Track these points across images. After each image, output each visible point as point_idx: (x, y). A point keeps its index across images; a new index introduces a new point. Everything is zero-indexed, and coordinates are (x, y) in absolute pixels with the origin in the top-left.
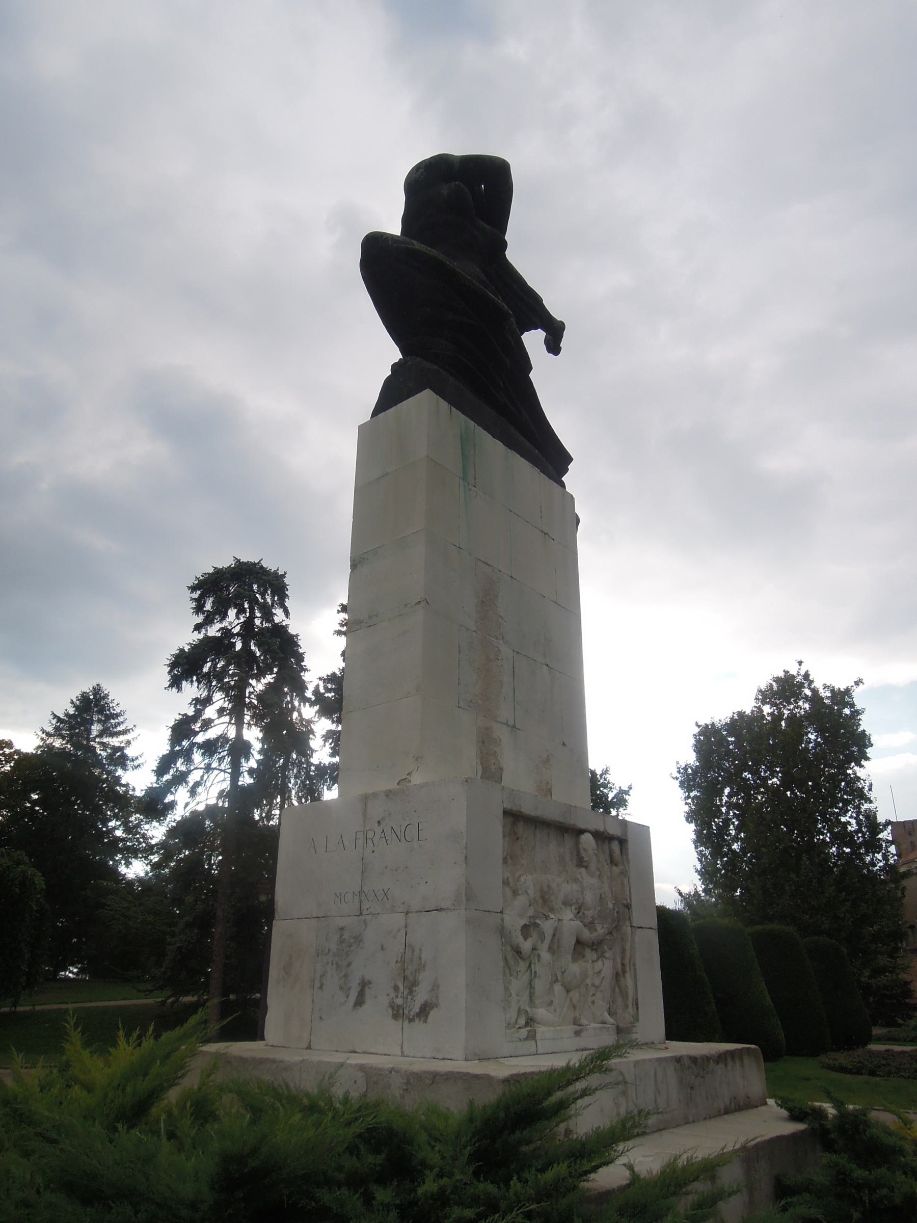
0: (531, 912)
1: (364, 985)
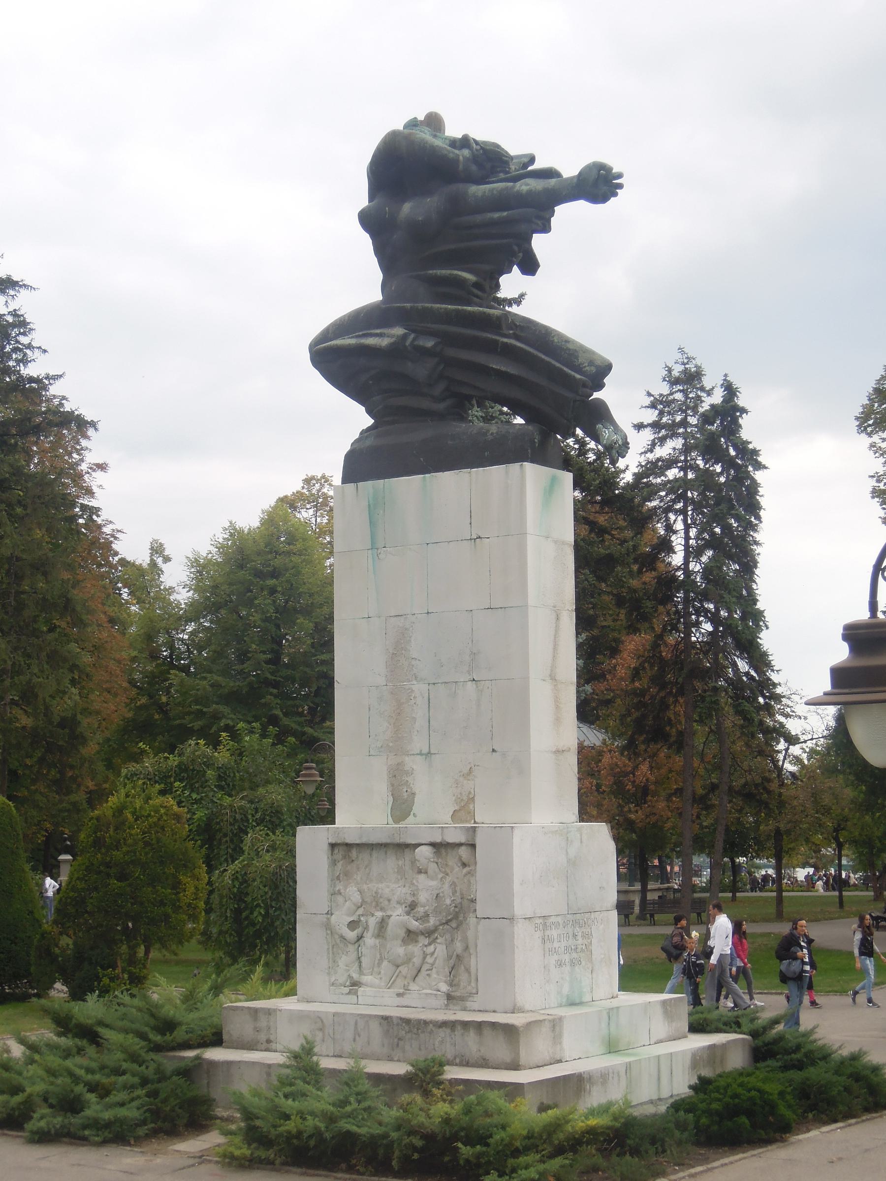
0: (360, 911)
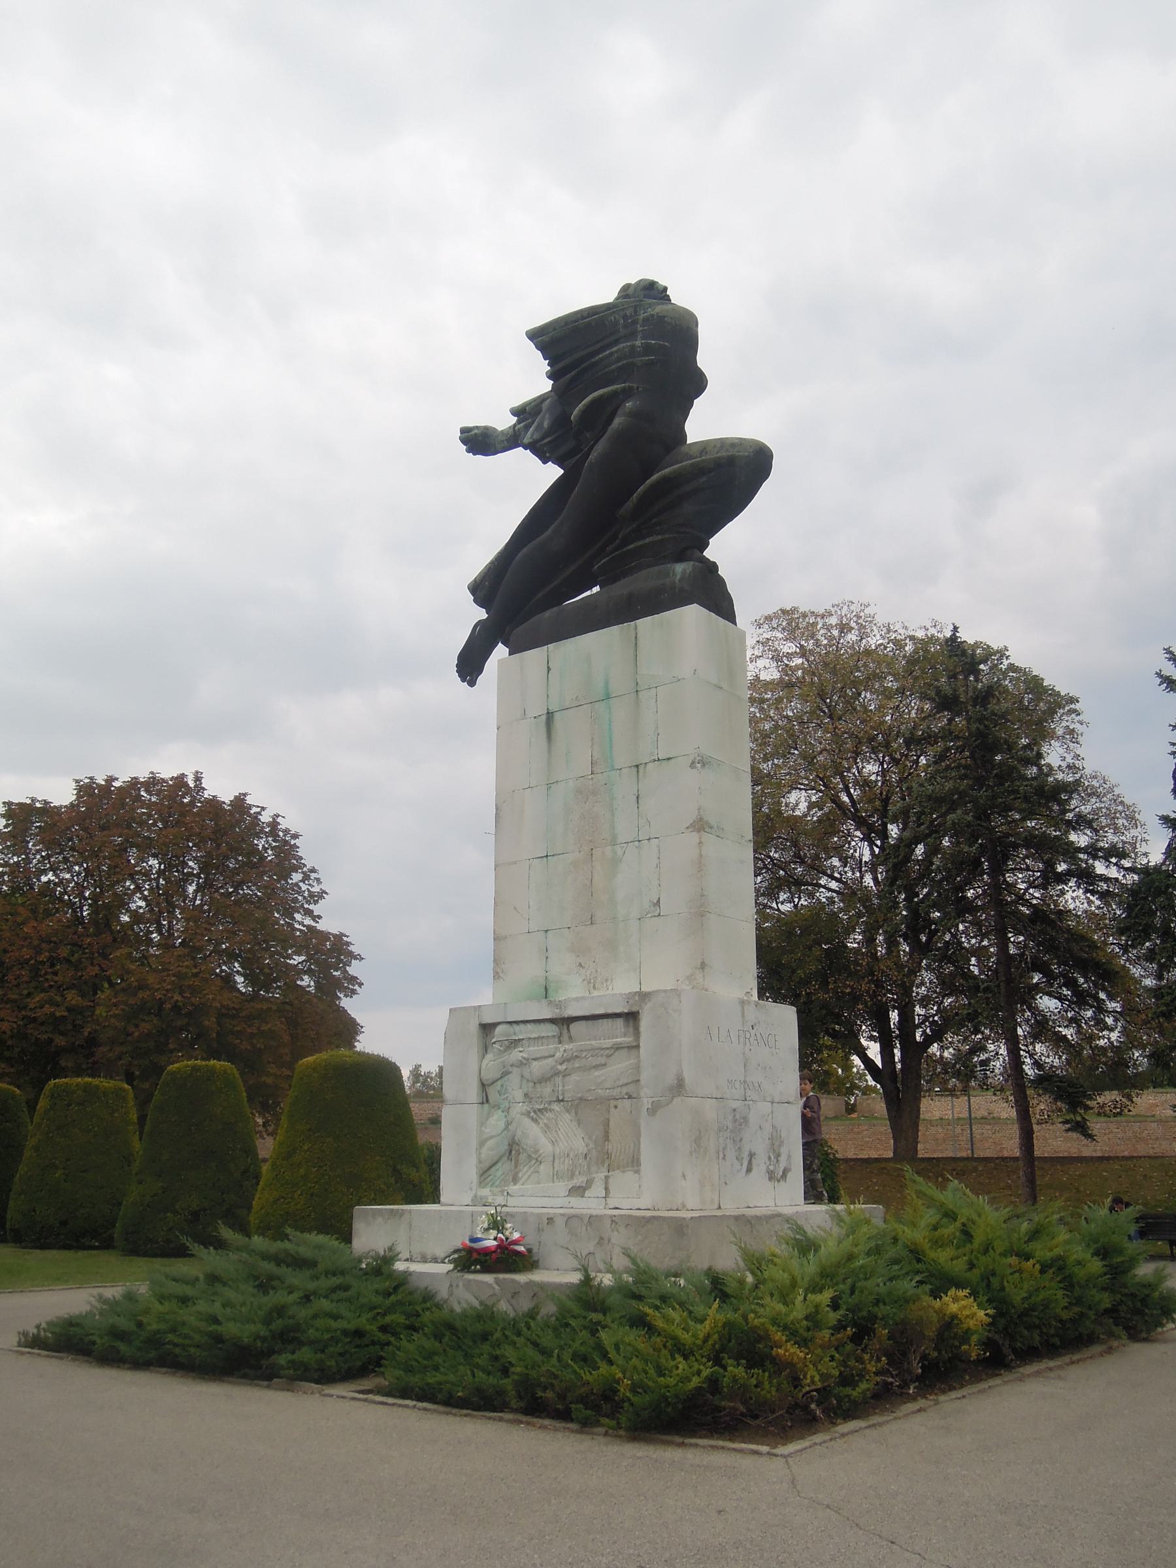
1: (752, 1155)
